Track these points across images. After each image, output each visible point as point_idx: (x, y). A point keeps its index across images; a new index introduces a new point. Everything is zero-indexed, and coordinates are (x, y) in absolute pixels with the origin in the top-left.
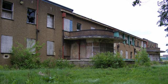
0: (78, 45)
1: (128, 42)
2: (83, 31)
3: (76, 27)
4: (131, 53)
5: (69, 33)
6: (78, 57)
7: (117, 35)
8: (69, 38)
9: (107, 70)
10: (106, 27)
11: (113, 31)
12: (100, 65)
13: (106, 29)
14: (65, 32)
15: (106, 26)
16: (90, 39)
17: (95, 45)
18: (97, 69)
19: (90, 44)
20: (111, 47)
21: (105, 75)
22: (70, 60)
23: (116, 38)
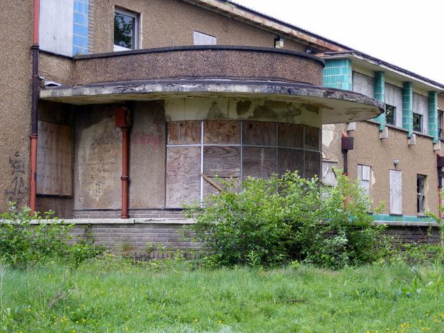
0: (119, 133)
1: (404, 120)
2: (152, 56)
3: (110, 32)
4: (421, 180)
5: (66, 66)
6: (118, 204)
7: (341, 80)
8: (67, 93)
9: (285, 278)
10: (278, 36)
11: (321, 56)
12: (245, 246)
13: (281, 45)
14: (43, 59)
15: (277, 26)
16: (186, 99)
17: (218, 135)
18: (224, 271)
19: (190, 128)
20: (306, 148)
21: (271, 307)
22: (72, 217)
23: (337, 95)
